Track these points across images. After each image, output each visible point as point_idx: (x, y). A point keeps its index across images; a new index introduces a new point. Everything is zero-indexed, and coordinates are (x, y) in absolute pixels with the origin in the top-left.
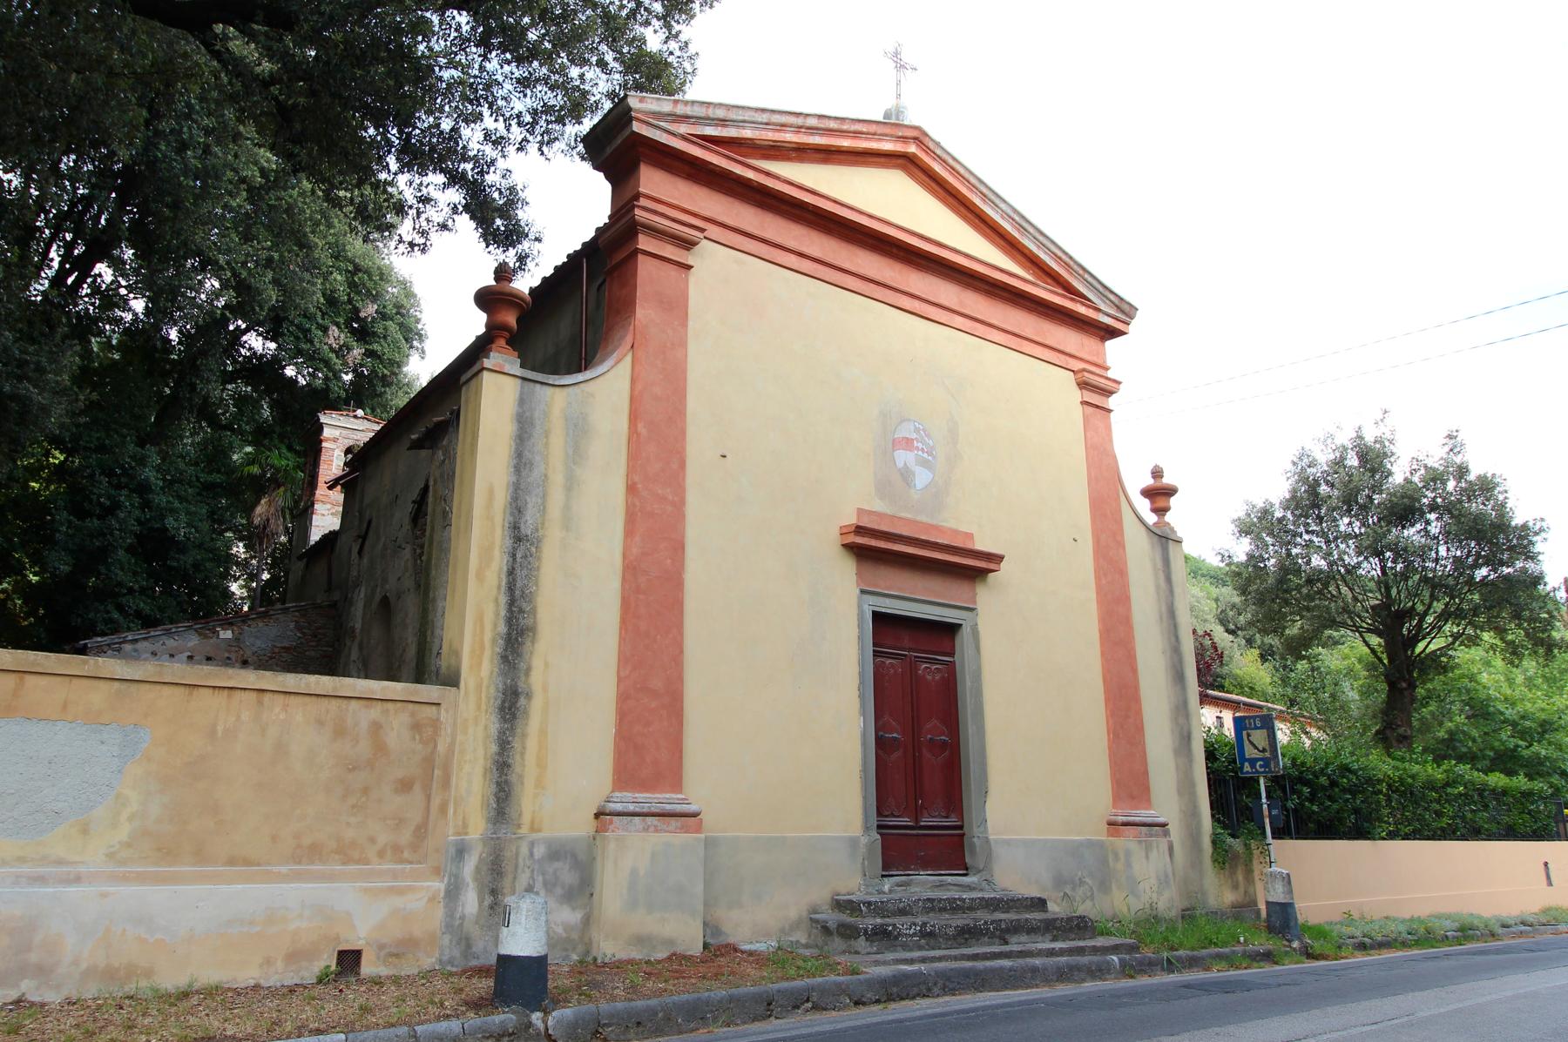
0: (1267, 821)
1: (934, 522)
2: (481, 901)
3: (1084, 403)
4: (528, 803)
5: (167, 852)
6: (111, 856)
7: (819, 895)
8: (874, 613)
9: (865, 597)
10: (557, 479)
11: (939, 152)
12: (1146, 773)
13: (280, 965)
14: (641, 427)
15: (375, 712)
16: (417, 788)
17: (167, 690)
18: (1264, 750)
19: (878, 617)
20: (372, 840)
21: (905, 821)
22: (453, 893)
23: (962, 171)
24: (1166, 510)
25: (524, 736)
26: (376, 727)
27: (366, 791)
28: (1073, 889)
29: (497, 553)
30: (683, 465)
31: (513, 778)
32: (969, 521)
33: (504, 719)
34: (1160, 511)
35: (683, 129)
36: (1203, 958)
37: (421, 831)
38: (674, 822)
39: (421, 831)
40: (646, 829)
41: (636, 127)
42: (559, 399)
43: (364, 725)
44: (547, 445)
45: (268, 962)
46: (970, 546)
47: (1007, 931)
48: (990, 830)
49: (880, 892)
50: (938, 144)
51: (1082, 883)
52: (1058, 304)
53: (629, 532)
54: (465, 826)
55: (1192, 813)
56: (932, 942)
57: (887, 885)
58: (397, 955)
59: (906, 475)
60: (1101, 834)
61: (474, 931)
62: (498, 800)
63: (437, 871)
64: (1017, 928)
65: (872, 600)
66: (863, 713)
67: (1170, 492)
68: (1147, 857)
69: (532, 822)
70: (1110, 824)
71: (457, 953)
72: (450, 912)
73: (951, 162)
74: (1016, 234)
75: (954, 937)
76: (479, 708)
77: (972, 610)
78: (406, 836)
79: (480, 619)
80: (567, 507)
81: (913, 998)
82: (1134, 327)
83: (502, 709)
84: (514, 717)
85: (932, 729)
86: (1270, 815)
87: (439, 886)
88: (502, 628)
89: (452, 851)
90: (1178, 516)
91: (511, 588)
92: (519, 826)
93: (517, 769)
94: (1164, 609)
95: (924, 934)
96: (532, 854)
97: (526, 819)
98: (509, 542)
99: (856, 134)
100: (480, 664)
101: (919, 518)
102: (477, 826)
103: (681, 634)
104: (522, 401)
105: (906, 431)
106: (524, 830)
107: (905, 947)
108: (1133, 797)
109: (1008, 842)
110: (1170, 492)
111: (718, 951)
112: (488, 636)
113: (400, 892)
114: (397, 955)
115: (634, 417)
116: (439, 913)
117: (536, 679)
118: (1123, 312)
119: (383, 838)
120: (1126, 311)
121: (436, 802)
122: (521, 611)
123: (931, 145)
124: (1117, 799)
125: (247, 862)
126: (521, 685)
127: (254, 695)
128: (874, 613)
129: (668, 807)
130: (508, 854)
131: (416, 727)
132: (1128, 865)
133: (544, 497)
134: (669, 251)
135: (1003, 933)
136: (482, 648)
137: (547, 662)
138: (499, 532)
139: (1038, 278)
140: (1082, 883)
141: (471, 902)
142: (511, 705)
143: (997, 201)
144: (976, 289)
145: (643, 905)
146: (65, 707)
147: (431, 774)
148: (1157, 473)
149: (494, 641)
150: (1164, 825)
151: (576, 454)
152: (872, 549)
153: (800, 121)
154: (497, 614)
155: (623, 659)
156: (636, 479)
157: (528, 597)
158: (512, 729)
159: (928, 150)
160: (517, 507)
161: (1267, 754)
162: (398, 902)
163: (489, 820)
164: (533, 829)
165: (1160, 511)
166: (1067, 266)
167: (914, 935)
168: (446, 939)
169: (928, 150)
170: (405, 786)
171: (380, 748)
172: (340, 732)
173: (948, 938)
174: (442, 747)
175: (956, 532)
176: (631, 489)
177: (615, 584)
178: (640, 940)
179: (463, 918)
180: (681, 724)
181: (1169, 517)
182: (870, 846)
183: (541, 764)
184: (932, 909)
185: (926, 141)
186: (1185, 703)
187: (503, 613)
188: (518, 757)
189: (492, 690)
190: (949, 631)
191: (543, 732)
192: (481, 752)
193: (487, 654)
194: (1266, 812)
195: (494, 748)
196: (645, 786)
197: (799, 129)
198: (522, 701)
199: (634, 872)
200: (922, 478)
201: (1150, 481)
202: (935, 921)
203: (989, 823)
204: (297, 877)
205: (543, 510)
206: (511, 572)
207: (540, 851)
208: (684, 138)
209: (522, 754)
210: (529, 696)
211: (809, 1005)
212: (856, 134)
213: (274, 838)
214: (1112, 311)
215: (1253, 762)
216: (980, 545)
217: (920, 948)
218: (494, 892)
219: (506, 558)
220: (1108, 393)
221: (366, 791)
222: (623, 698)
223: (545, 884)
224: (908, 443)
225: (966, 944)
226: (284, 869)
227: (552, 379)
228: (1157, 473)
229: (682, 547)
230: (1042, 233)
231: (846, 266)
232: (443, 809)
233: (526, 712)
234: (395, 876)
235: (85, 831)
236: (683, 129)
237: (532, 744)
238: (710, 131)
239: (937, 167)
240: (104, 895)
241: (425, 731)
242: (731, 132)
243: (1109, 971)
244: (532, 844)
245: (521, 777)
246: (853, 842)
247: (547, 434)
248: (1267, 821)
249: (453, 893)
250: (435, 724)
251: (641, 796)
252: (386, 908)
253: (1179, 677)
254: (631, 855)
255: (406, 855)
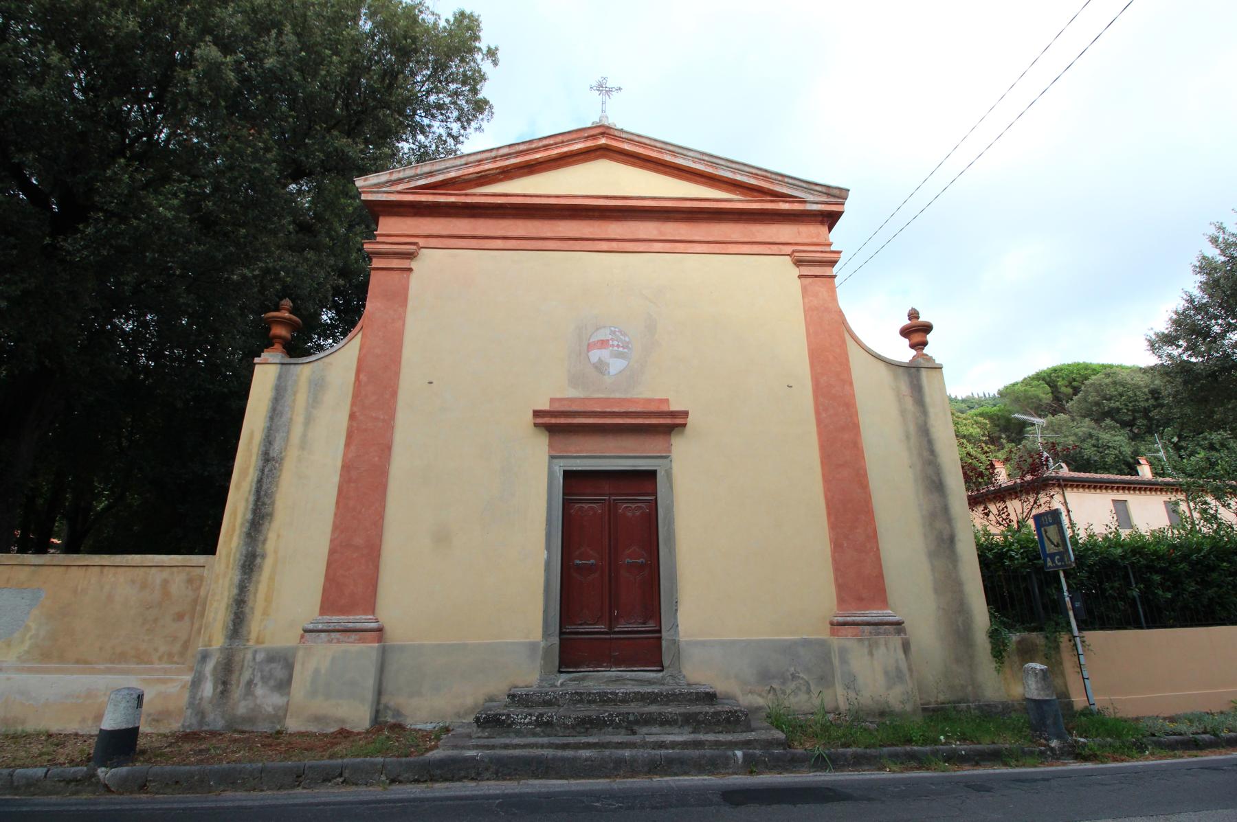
0: (1071, 613)
1: (629, 396)
2: (215, 689)
3: (800, 276)
4: (255, 625)
5: (46, 656)
6: (19, 658)
7: (497, 686)
8: (565, 472)
9: (556, 461)
10: (299, 419)
11: (624, 135)
12: (881, 576)
13: (90, 722)
14: (363, 377)
15: (165, 574)
16: (187, 618)
17: (56, 569)
18: (1057, 546)
19: (568, 475)
20: (156, 650)
21: (601, 627)
22: (196, 683)
23: (648, 142)
24: (925, 344)
25: (258, 582)
26: (165, 583)
27: (156, 620)
28: (784, 683)
29: (251, 470)
30: (394, 394)
31: (247, 610)
32: (658, 388)
33: (244, 573)
34: (919, 345)
35: (400, 187)
36: (881, 756)
37: (186, 645)
38: (353, 636)
39: (186, 645)
40: (330, 641)
41: (363, 197)
42: (304, 371)
43: (158, 581)
44: (294, 401)
45: (84, 720)
46: (664, 408)
47: (637, 722)
48: (681, 633)
49: (553, 686)
50: (621, 131)
51: (794, 677)
52: (783, 212)
53: (347, 445)
54: (210, 641)
55: (957, 610)
56: (549, 730)
57: (563, 678)
58: (157, 721)
59: (600, 367)
60: (824, 634)
61: (207, 707)
62: (234, 624)
63: (191, 669)
64: (647, 720)
65: (562, 462)
66: (548, 547)
67: (927, 328)
68: (871, 654)
69: (258, 638)
70: (832, 624)
71: (194, 721)
72: (193, 697)
73: (636, 139)
74: (710, 170)
75: (573, 727)
76: (227, 567)
77: (667, 457)
78: (177, 647)
79: (234, 513)
80: (304, 436)
81: (460, 780)
82: (849, 207)
83: (243, 566)
84: (252, 570)
85: (631, 556)
86: (1074, 609)
87: (188, 678)
88: (249, 516)
89: (199, 656)
90: (935, 347)
91: (258, 491)
92: (248, 640)
93: (250, 604)
94: (912, 428)
95: (538, 723)
96: (254, 659)
97: (253, 635)
98: (261, 463)
99: (547, 147)
100: (231, 539)
101: (612, 396)
102: (218, 640)
103: (384, 507)
104: (280, 377)
105: (603, 335)
106: (251, 643)
107: (518, 733)
108: (861, 599)
109: (696, 643)
110: (927, 328)
111: (386, 726)
112: (239, 521)
113: (164, 682)
114: (157, 721)
115: (359, 371)
116: (186, 696)
117: (270, 546)
118: (834, 196)
119: (163, 648)
120: (840, 195)
121: (196, 626)
122: (264, 504)
123: (617, 133)
124: (841, 601)
125: (86, 662)
126: (259, 550)
127: (98, 569)
128: (565, 472)
129: (350, 625)
130: (237, 659)
131: (190, 581)
132: (844, 661)
133: (288, 432)
134: (396, 263)
135: (631, 724)
136: (234, 530)
137: (277, 537)
138: (254, 458)
139: (746, 195)
140: (794, 677)
141: (208, 689)
142: (250, 564)
143: (685, 152)
144: (676, 220)
145: (325, 693)
146: (8, 580)
147: (196, 608)
148: (913, 315)
149: (242, 524)
150: (899, 623)
151: (315, 399)
152: (557, 425)
153: (493, 154)
154: (246, 508)
155: (335, 527)
156: (355, 409)
157: (269, 495)
158: (250, 579)
159: (616, 138)
160: (268, 440)
161: (1061, 549)
162: (161, 688)
163: (227, 637)
164: (258, 641)
165: (919, 345)
166: (766, 178)
167: (529, 723)
168: (189, 711)
169: (616, 138)
170: (180, 617)
171: (166, 594)
172: (144, 586)
173: (566, 727)
174: (202, 593)
175: (649, 401)
176: (352, 416)
177: (336, 479)
178: (317, 719)
179: (201, 699)
180: (377, 568)
181: (926, 350)
182: (547, 651)
183: (268, 600)
184: (581, 701)
185: (612, 132)
186: (946, 510)
187: (251, 506)
188: (251, 596)
189: (238, 556)
190: (652, 475)
191: (272, 579)
192: (226, 594)
193: (237, 532)
194: (1069, 605)
195: (235, 591)
196: (342, 611)
197: (494, 159)
198: (259, 560)
199: (317, 672)
200: (616, 366)
201: (906, 322)
202: (549, 713)
203: (680, 627)
204: (109, 671)
205: (287, 440)
206: (260, 481)
207: (260, 657)
208: (399, 192)
209: (255, 594)
210: (263, 556)
211: (341, 780)
212: (547, 147)
213: (101, 649)
214: (824, 199)
215: (1052, 556)
216: (674, 407)
217: (535, 735)
218: (224, 683)
219: (257, 473)
220: (833, 263)
221: (156, 620)
222: (332, 552)
223: (262, 678)
224: (603, 344)
225: (587, 733)
226: (102, 667)
227: (300, 360)
228: (913, 315)
229: (389, 448)
230: (732, 162)
231: (549, 235)
232: (200, 630)
233: (260, 567)
234: (165, 671)
235: (9, 645)
236: (400, 187)
237: (263, 588)
238: (413, 184)
239: (626, 147)
240: (8, 679)
241: (194, 583)
242: (440, 178)
243: (726, 765)
244: (255, 652)
245: (252, 608)
246: (533, 646)
247: (295, 394)
248: (1071, 613)
249: (196, 683)
250: (201, 578)
251: (335, 618)
252: (166, 694)
253: (935, 485)
254: (317, 660)
255: (176, 659)
